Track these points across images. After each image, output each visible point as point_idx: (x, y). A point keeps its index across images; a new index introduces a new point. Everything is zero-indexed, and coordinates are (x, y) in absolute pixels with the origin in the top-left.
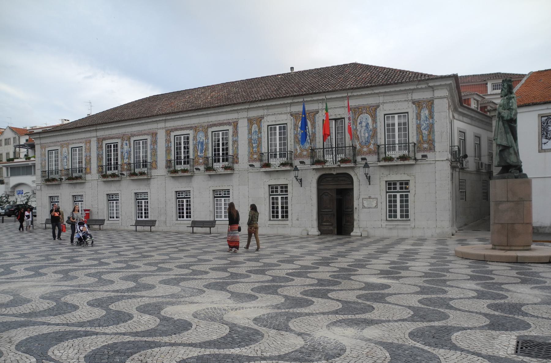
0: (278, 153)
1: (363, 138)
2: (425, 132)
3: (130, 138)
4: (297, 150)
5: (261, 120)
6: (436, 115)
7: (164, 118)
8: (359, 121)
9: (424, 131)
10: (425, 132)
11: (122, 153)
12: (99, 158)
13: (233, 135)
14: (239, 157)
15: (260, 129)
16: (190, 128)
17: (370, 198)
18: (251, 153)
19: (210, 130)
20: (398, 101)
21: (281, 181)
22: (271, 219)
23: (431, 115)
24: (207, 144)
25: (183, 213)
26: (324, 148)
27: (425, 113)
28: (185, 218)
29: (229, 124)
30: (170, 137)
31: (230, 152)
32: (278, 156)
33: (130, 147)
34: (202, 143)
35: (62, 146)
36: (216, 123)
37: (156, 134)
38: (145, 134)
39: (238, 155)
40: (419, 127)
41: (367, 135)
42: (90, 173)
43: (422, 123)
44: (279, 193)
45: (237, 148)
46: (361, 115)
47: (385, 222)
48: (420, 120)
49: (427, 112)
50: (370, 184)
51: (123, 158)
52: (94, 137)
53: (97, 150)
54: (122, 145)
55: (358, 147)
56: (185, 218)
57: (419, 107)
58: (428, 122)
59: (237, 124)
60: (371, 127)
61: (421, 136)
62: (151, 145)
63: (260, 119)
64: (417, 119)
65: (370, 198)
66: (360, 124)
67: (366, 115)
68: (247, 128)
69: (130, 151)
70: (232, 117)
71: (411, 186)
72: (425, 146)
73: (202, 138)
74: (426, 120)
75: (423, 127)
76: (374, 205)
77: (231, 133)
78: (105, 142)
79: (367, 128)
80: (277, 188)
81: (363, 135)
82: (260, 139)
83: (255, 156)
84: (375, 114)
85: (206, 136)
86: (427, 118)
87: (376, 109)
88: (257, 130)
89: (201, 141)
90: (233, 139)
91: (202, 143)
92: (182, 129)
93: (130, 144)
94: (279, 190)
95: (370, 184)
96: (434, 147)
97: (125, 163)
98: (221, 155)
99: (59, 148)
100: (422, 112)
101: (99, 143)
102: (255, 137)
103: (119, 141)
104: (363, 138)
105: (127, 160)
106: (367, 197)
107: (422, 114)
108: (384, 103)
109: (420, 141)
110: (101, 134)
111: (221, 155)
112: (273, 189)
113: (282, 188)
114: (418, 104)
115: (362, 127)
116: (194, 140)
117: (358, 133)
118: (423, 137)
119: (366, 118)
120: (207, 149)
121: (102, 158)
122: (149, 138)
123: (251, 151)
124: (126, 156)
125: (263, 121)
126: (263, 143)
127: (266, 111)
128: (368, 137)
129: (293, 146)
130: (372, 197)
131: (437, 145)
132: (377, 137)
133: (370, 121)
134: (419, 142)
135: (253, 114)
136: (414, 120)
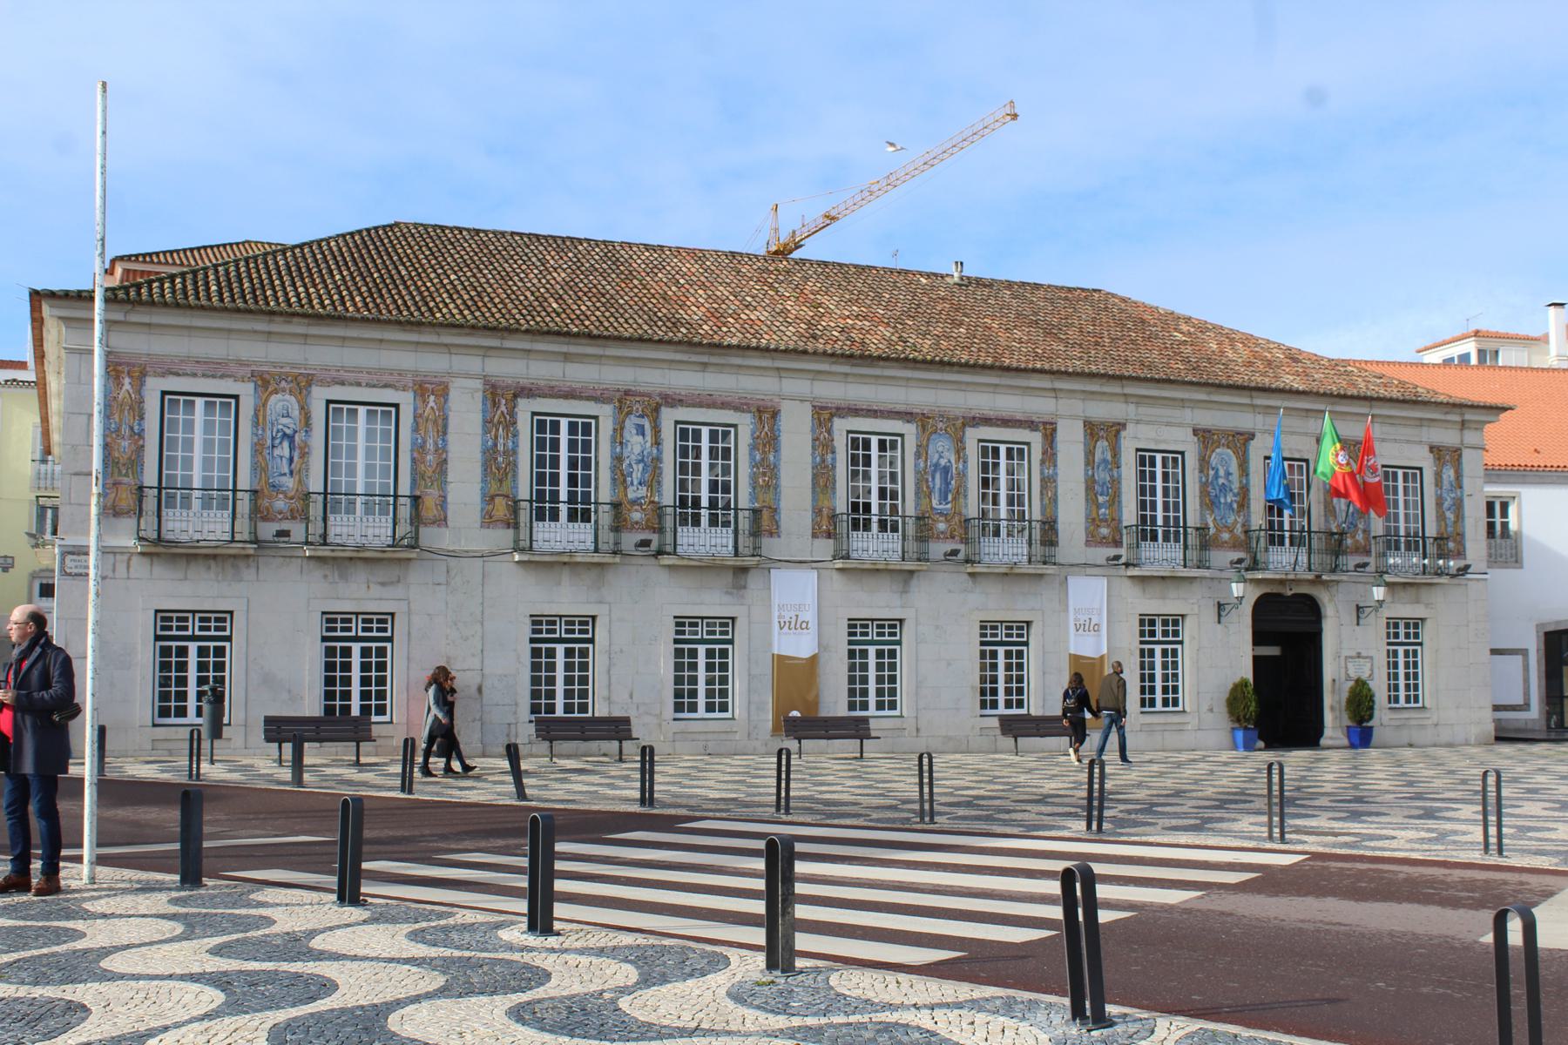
0: (1287, 534)
2: (1450, 516)
3: (657, 410)
5: (1118, 432)
6: (1466, 482)
7: (564, 349)
11: (618, 459)
12: (497, 466)
13: (1043, 462)
14: (1060, 526)
15: (1116, 452)
16: (907, 416)
17: (1359, 656)
18: (1093, 522)
19: (973, 436)
20: (1408, 442)
21: (1170, 607)
22: (1180, 708)
24: (962, 475)
25: (865, 693)
26: (325, 493)
27: (1449, 474)
28: (702, 712)
29: (1031, 425)
30: (829, 432)
31: (744, 497)
32: (1287, 541)
33: (657, 443)
34: (946, 470)
35: (265, 382)
36: (992, 414)
37: (775, 414)
38: (724, 405)
40: (1439, 503)
42: (442, 521)
44: (1159, 637)
45: (1054, 500)
49: (1452, 473)
51: (620, 478)
52: (468, 376)
53: (486, 431)
54: (619, 429)
56: (702, 712)
59: (1054, 430)
62: (753, 448)
63: (1115, 430)
65: (1359, 656)
68: (1082, 447)
69: (658, 459)
70: (432, 363)
71: (1427, 634)
73: (946, 454)
75: (1446, 505)
77: (606, 427)
78: (525, 409)
80: (1152, 623)
82: (1116, 483)
83: (1104, 531)
85: (960, 450)
89: (943, 462)
90: (1042, 473)
91: (946, 470)
92: (570, 395)
93: (657, 431)
94: (1159, 628)
97: (634, 502)
98: (563, 496)
99: (246, 390)
101: (495, 405)
102: (1102, 475)
103: (605, 412)
105: (643, 491)
108: (1138, 422)
110: (509, 369)
111: (563, 496)
112: (1147, 624)
113: (1165, 623)
114: (1205, 436)
116: (918, 455)
119: (1224, 458)
120: (961, 492)
121: (514, 465)
122: (745, 425)
124: (637, 476)
125: (1123, 434)
126: (1124, 498)
127: (1132, 407)
130: (1364, 654)
131: (1468, 545)
135: (1103, 411)
136: (1433, 487)
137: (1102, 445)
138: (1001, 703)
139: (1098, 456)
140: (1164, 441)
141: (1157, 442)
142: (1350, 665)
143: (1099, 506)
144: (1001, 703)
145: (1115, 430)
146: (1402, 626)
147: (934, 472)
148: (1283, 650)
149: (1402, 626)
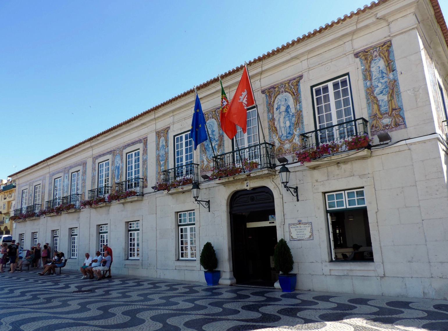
1: (283, 129)
2: (383, 98)
4: (203, 161)
5: (167, 131)
6: (399, 65)
8: (276, 106)
9: (380, 97)
10: (383, 98)
13: (143, 154)
14: (148, 179)
15: (167, 141)
17: (300, 222)
23: (391, 67)
27: (380, 64)
29: (140, 141)
33: (68, 180)
39: (147, 177)
40: (370, 92)
41: (288, 124)
43: (375, 83)
45: (146, 169)
46: (279, 97)
47: (328, 264)
48: (371, 80)
49: (381, 64)
50: (298, 200)
55: (277, 144)
57: (366, 59)
58: (386, 80)
60: (293, 110)
61: (375, 107)
63: (166, 130)
64: (365, 79)
65: (300, 222)
66: (277, 109)
67: (285, 94)
68: (155, 143)
69: (68, 185)
72: (386, 121)
74: (383, 77)
75: (377, 91)
76: (307, 234)
79: (288, 112)
81: (282, 125)
82: (167, 153)
84: (298, 90)
86: (382, 73)
87: (298, 82)
88: (164, 144)
89: (118, 165)
93: (69, 176)
95: (298, 200)
96: (403, 119)
100: (373, 65)
101: (50, 179)
104: (283, 129)
106: (297, 222)
107: (373, 69)
109: (375, 115)
115: (280, 113)
116: (112, 165)
117: (276, 123)
118: (379, 106)
123: (159, 171)
128: (290, 127)
129: (199, 157)
130: (304, 221)
132: (302, 123)
133: (291, 102)
134: (374, 116)
136: (361, 83)
137: (162, 139)
138: (136, 254)
139: (161, 144)
140: (183, 128)
141: (181, 129)
142: (292, 230)
143: (161, 167)
144: (136, 254)
145: (166, 130)
146: (345, 194)
147: (116, 169)
148: (246, 225)
149: (345, 194)
